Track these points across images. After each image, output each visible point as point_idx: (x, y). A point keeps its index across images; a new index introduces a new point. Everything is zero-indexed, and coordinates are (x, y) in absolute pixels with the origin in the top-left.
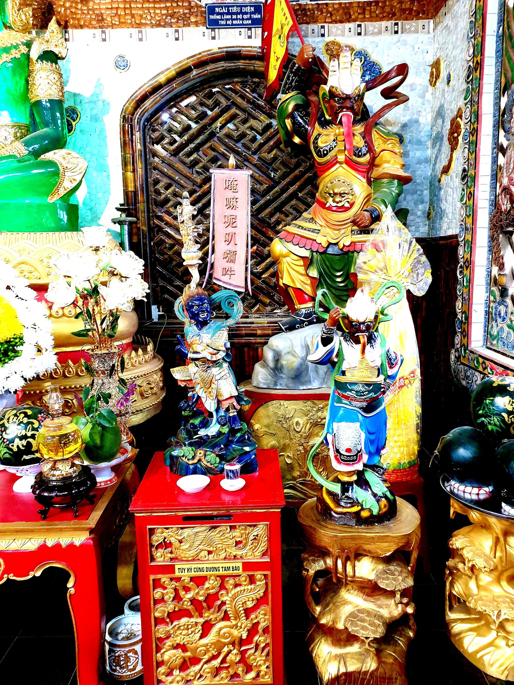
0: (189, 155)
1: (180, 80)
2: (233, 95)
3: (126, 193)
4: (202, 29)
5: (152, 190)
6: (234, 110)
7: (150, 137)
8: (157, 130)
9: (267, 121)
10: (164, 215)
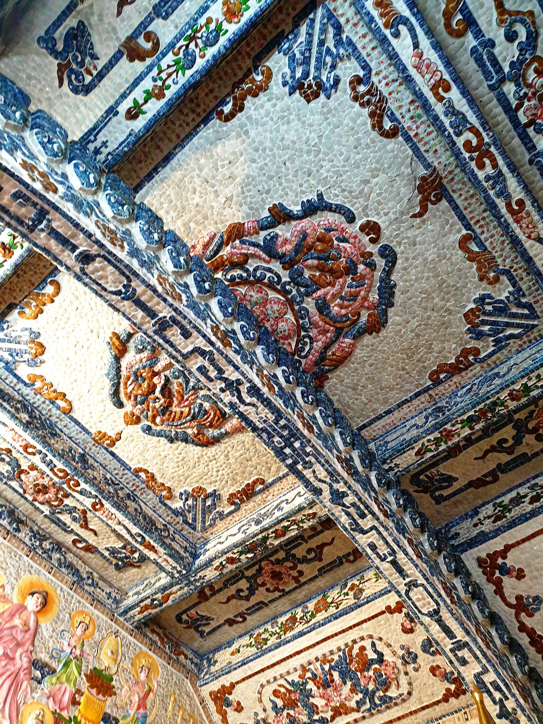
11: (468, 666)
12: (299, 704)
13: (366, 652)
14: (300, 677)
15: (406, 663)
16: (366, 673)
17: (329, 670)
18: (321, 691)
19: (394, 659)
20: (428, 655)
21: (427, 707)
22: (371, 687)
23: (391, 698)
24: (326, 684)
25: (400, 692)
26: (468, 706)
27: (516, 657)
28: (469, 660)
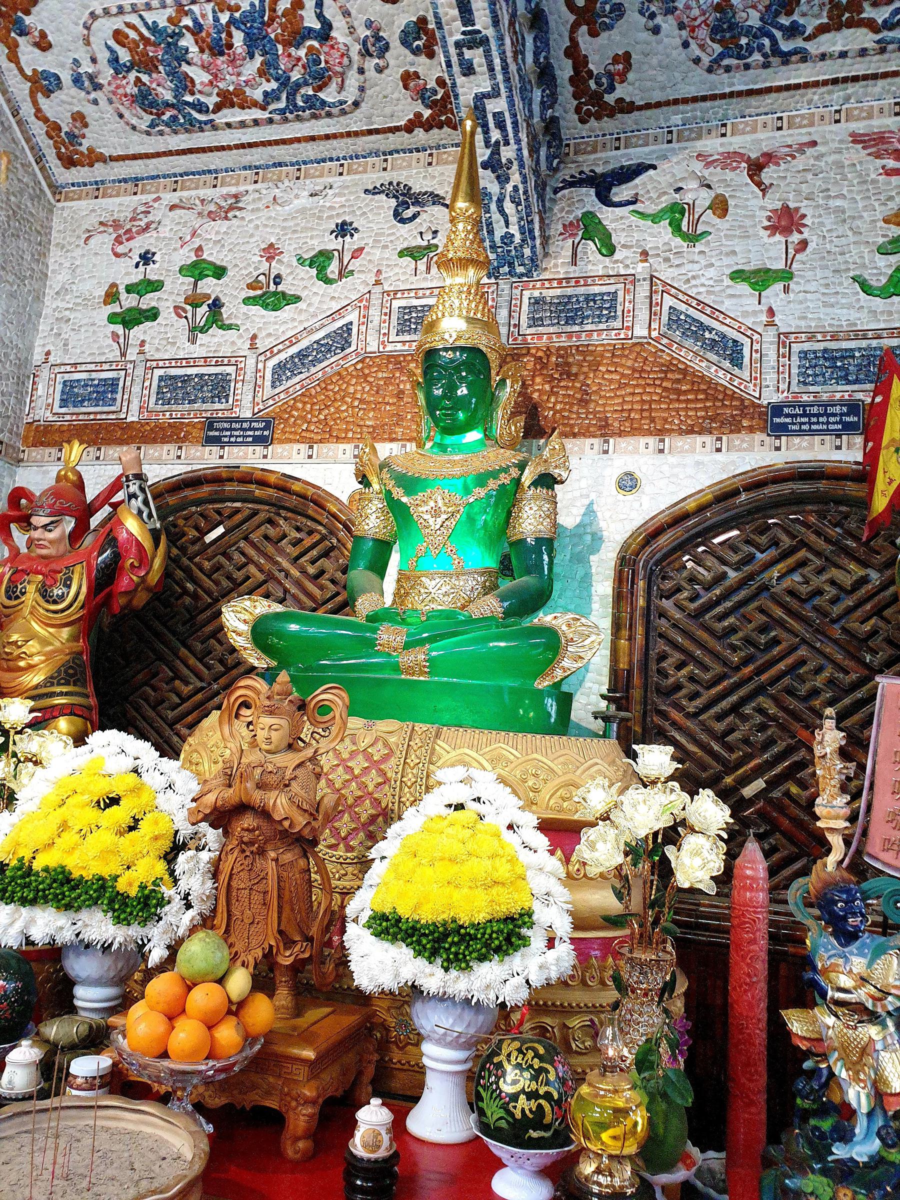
1: (716, 508)
2: (803, 530)
3: (614, 672)
4: (759, 436)
5: (654, 668)
6: (803, 553)
9: (861, 572)
10: (670, 709)
11: (472, 77)
12: (161, 68)
13: (302, 13)
14: (170, 20)
15: (366, 53)
16: (292, 50)
17: (229, 23)
18: (205, 56)
19: (348, 40)
20: (407, 52)
21: (377, 131)
22: (295, 76)
23: (323, 103)
24: (218, 48)
25: (341, 97)
26: (438, 147)
27: (543, 91)
28: (477, 69)
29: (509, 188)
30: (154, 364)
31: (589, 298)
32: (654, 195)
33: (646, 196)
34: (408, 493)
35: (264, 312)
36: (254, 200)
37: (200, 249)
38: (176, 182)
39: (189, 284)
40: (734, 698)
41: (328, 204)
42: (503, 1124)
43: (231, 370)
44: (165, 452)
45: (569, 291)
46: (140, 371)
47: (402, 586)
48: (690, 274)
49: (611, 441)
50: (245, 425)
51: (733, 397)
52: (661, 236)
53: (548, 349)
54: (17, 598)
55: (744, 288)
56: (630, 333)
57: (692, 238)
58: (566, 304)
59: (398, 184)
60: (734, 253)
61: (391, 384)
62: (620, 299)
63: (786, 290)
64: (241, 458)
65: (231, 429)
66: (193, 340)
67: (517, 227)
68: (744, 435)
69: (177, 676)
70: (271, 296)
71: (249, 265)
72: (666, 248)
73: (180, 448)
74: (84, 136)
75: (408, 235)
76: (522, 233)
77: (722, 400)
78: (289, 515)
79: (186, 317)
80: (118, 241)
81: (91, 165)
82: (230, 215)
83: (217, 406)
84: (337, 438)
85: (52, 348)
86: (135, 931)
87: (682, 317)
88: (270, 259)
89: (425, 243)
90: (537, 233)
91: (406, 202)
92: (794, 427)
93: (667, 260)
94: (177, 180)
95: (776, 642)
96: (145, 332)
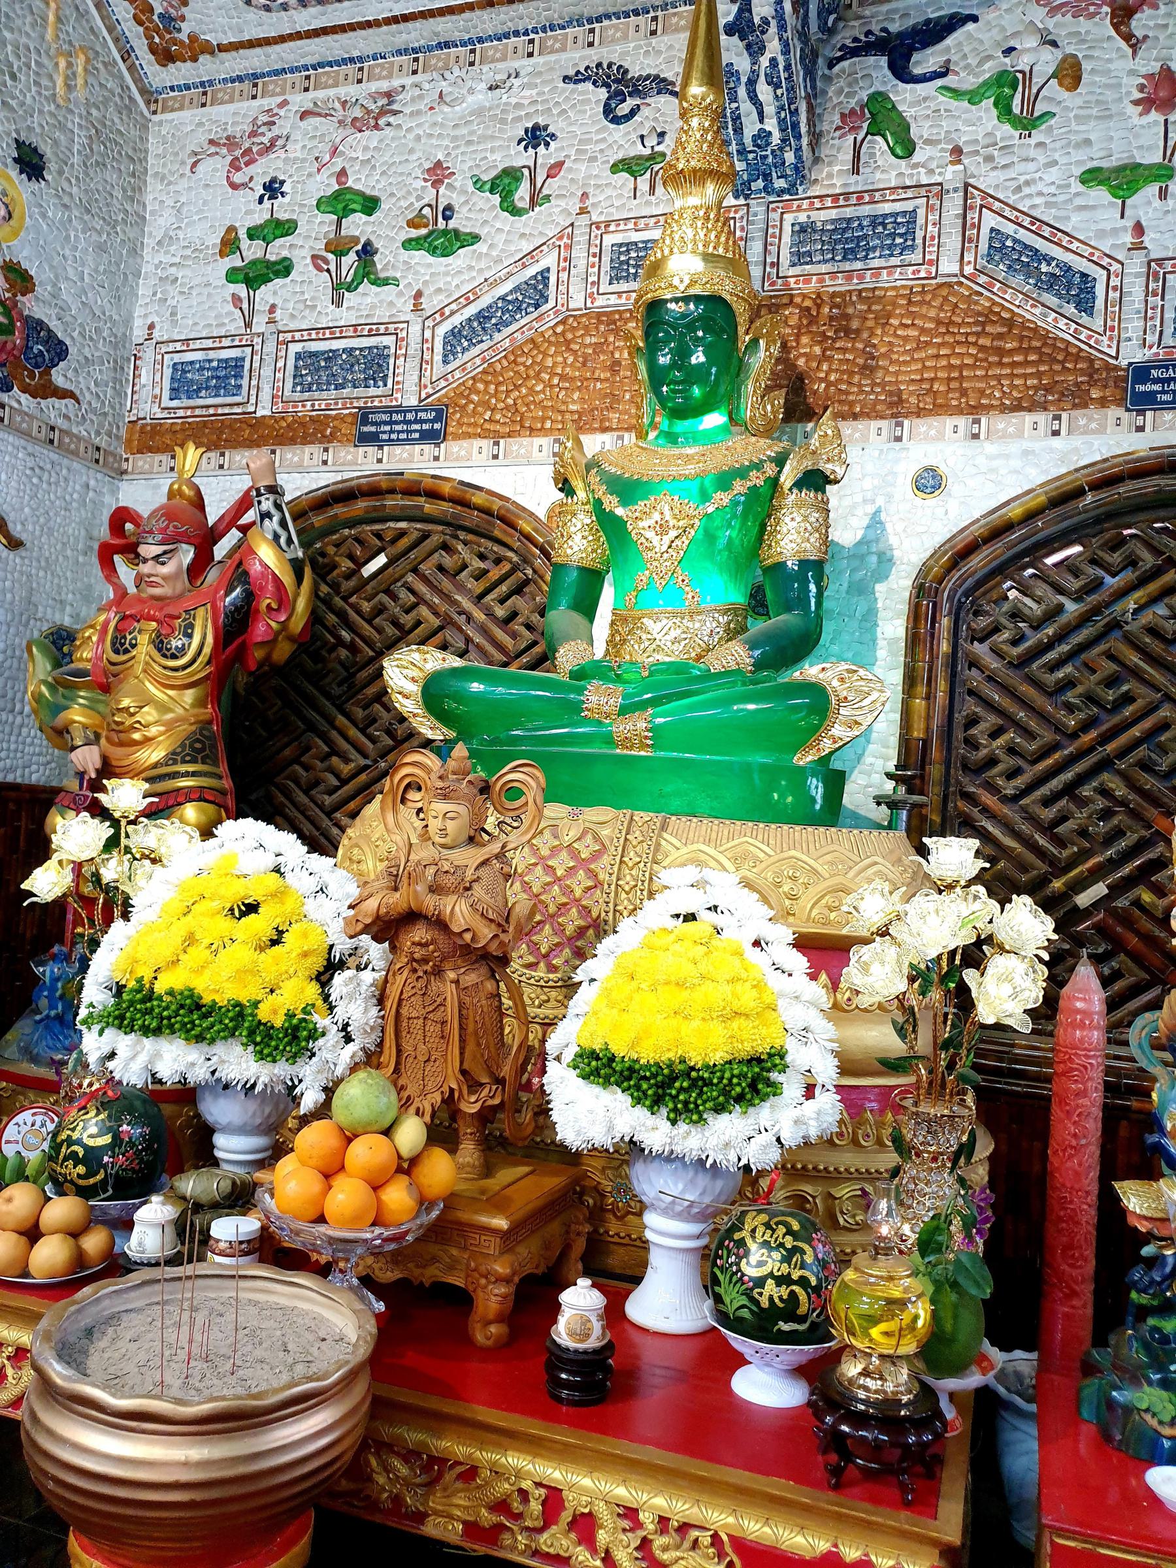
0: (1054, 667)
1: (1051, 515)
3: (905, 742)
4: (1114, 412)
5: (961, 736)
7: (969, 628)
8: (987, 613)
10: (980, 791)
29: (764, 61)
30: (289, 336)
31: (877, 221)
32: (972, 61)
33: (962, 64)
34: (624, 503)
35: (431, 259)
36: (413, 99)
37: (343, 173)
38: (308, 77)
39: (330, 224)
40: (1068, 775)
41: (514, 101)
42: (745, 1313)
43: (389, 341)
44: (307, 456)
45: (848, 212)
46: (270, 347)
47: (617, 631)
48: (1022, 179)
49: (906, 423)
50: (409, 416)
51: (1078, 356)
52: (981, 122)
53: (819, 295)
54: (126, 651)
55: (1100, 195)
56: (933, 270)
57: (1027, 123)
58: (844, 230)
59: (610, 66)
60: (1088, 142)
61: (603, 352)
62: (920, 221)
63: (1163, 194)
64: (405, 461)
65: (391, 423)
66: (338, 302)
67: (774, 121)
68: (1093, 412)
69: (335, 751)
70: (440, 236)
71: (409, 193)
72: (988, 141)
73: (326, 450)
74: (183, 18)
75: (624, 141)
76: (782, 130)
77: (1062, 362)
78: (470, 537)
79: (328, 271)
80: (235, 166)
81: (195, 59)
82: (381, 122)
83: (372, 391)
84: (531, 429)
85: (156, 319)
86: (282, 1070)
87: (1009, 243)
88: (436, 184)
89: (648, 151)
90: (803, 129)
91: (621, 90)
92: (1165, 397)
93: (989, 159)
94: (309, 74)
95: (1128, 699)
96: (275, 293)
